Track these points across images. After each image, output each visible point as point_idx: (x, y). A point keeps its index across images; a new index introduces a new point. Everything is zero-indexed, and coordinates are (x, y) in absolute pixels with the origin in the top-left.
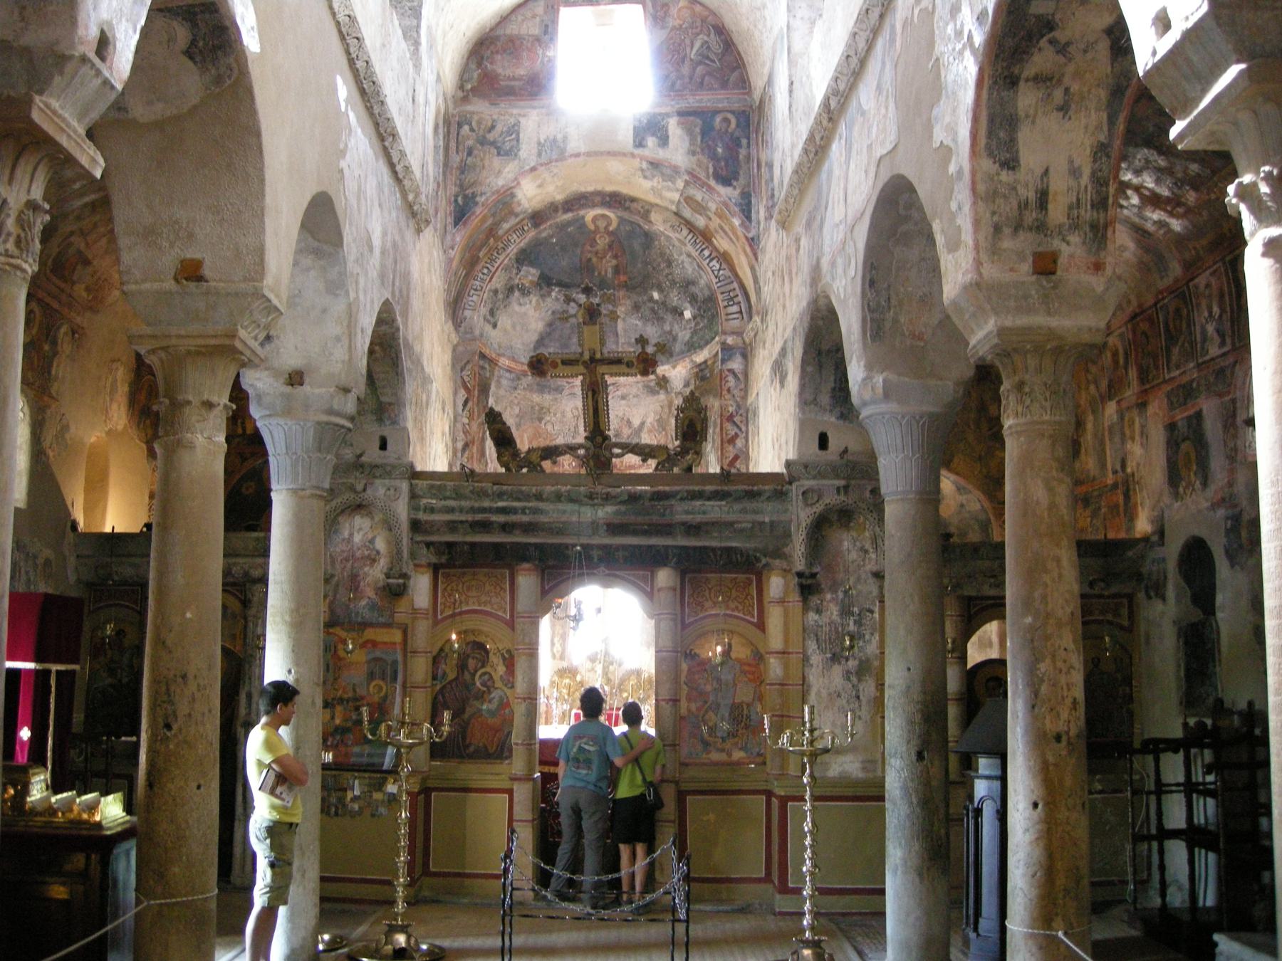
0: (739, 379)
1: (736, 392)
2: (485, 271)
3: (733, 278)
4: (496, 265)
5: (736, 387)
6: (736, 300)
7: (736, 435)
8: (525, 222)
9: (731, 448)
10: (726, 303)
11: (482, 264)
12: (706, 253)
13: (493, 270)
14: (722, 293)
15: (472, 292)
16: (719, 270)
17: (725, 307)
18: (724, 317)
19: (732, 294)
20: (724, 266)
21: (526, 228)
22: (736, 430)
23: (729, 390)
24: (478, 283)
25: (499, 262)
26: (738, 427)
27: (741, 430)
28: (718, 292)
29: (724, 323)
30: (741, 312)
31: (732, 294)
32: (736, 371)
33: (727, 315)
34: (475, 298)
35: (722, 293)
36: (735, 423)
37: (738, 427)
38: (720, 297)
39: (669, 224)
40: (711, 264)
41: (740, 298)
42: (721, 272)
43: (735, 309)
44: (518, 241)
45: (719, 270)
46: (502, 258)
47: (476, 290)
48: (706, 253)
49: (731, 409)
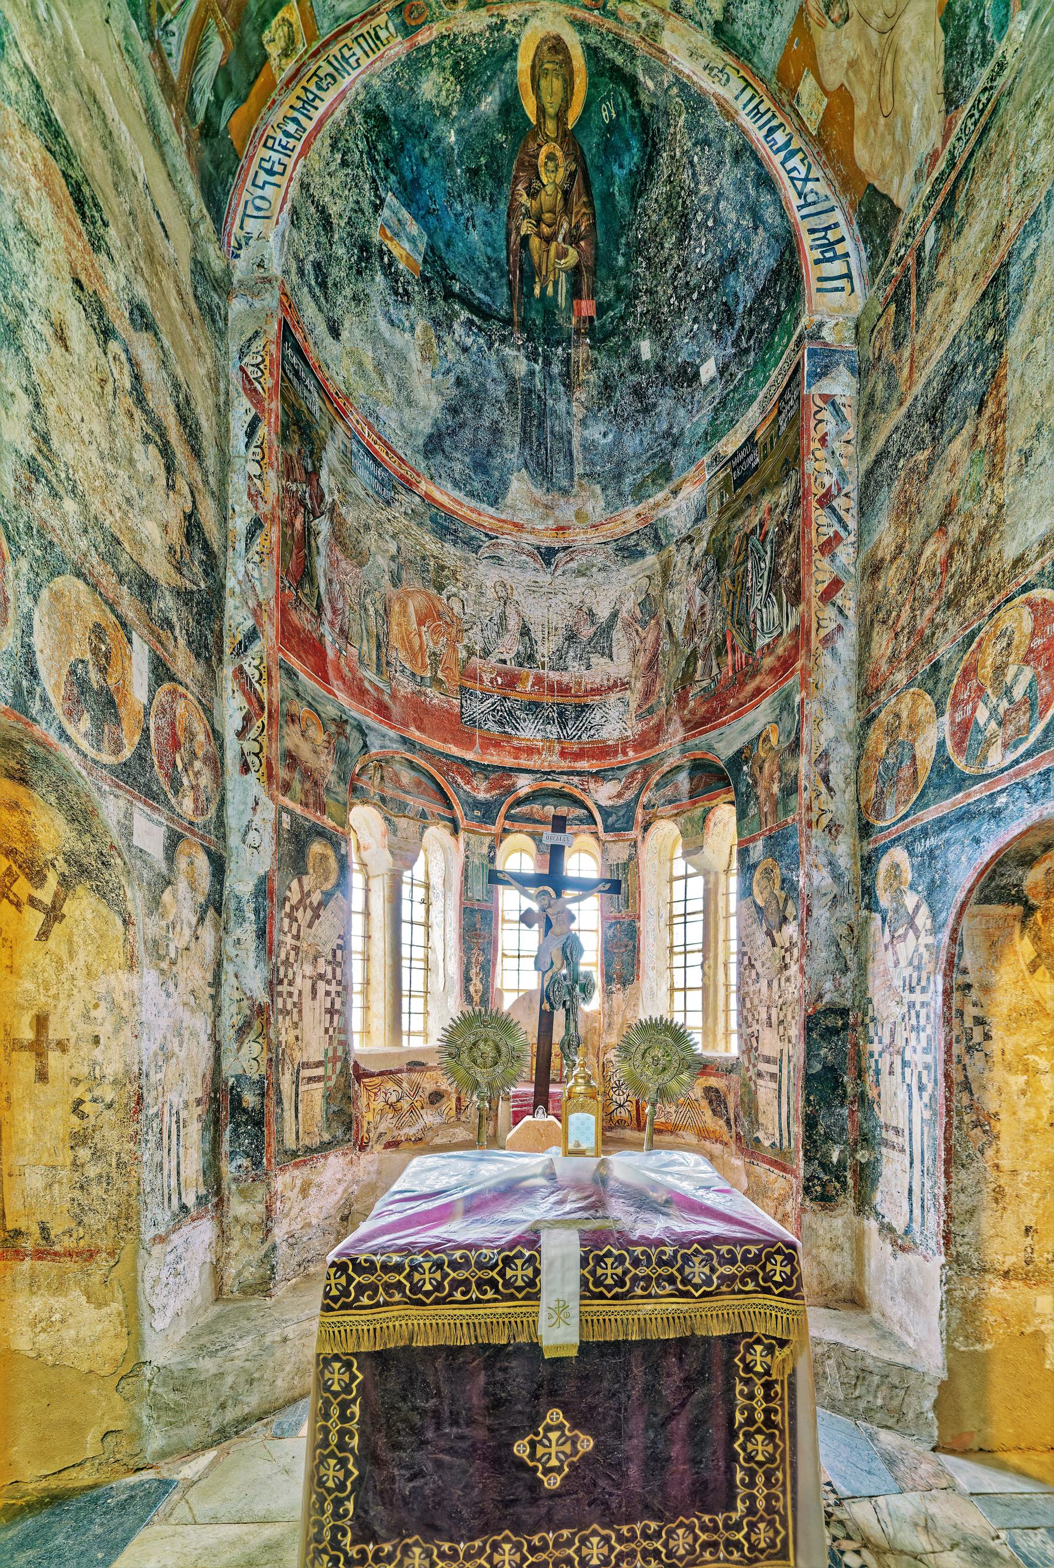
0: (844, 419)
1: (836, 445)
2: (291, 128)
3: (833, 202)
4: (316, 115)
5: (839, 434)
6: (840, 249)
7: (837, 537)
8: (381, 19)
9: (825, 563)
10: (817, 254)
11: (283, 110)
12: (780, 137)
13: (310, 125)
14: (812, 231)
15: (263, 177)
16: (806, 180)
17: (817, 262)
18: (815, 285)
19: (832, 236)
20: (815, 173)
21: (383, 34)
22: (837, 527)
23: (823, 440)
24: (276, 157)
25: (323, 107)
26: (840, 520)
27: (845, 527)
28: (803, 227)
29: (816, 297)
30: (848, 276)
31: (832, 236)
32: (839, 400)
33: (821, 279)
34: (269, 191)
35: (812, 231)
36: (833, 510)
37: (840, 520)
38: (807, 240)
39: (703, 62)
40: (789, 165)
41: (848, 246)
42: (810, 185)
43: (837, 268)
44: (365, 62)
45: (806, 180)
46: (330, 96)
47: (270, 172)
48: (780, 137)
49: (828, 480)
